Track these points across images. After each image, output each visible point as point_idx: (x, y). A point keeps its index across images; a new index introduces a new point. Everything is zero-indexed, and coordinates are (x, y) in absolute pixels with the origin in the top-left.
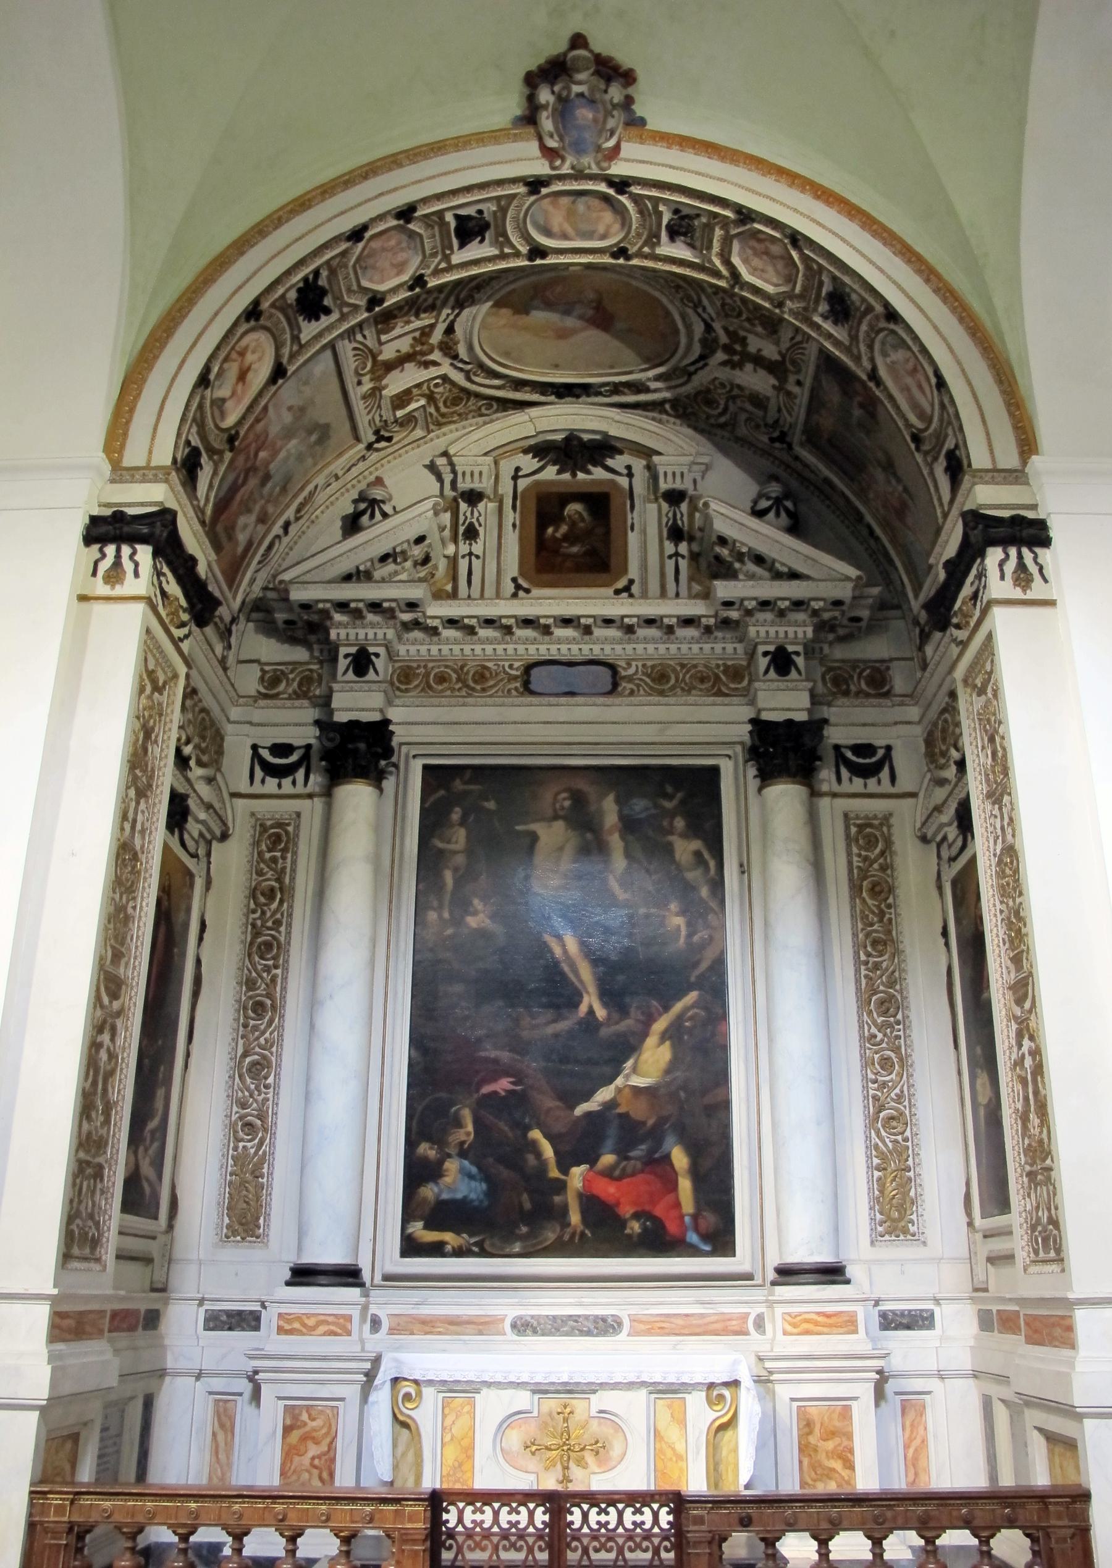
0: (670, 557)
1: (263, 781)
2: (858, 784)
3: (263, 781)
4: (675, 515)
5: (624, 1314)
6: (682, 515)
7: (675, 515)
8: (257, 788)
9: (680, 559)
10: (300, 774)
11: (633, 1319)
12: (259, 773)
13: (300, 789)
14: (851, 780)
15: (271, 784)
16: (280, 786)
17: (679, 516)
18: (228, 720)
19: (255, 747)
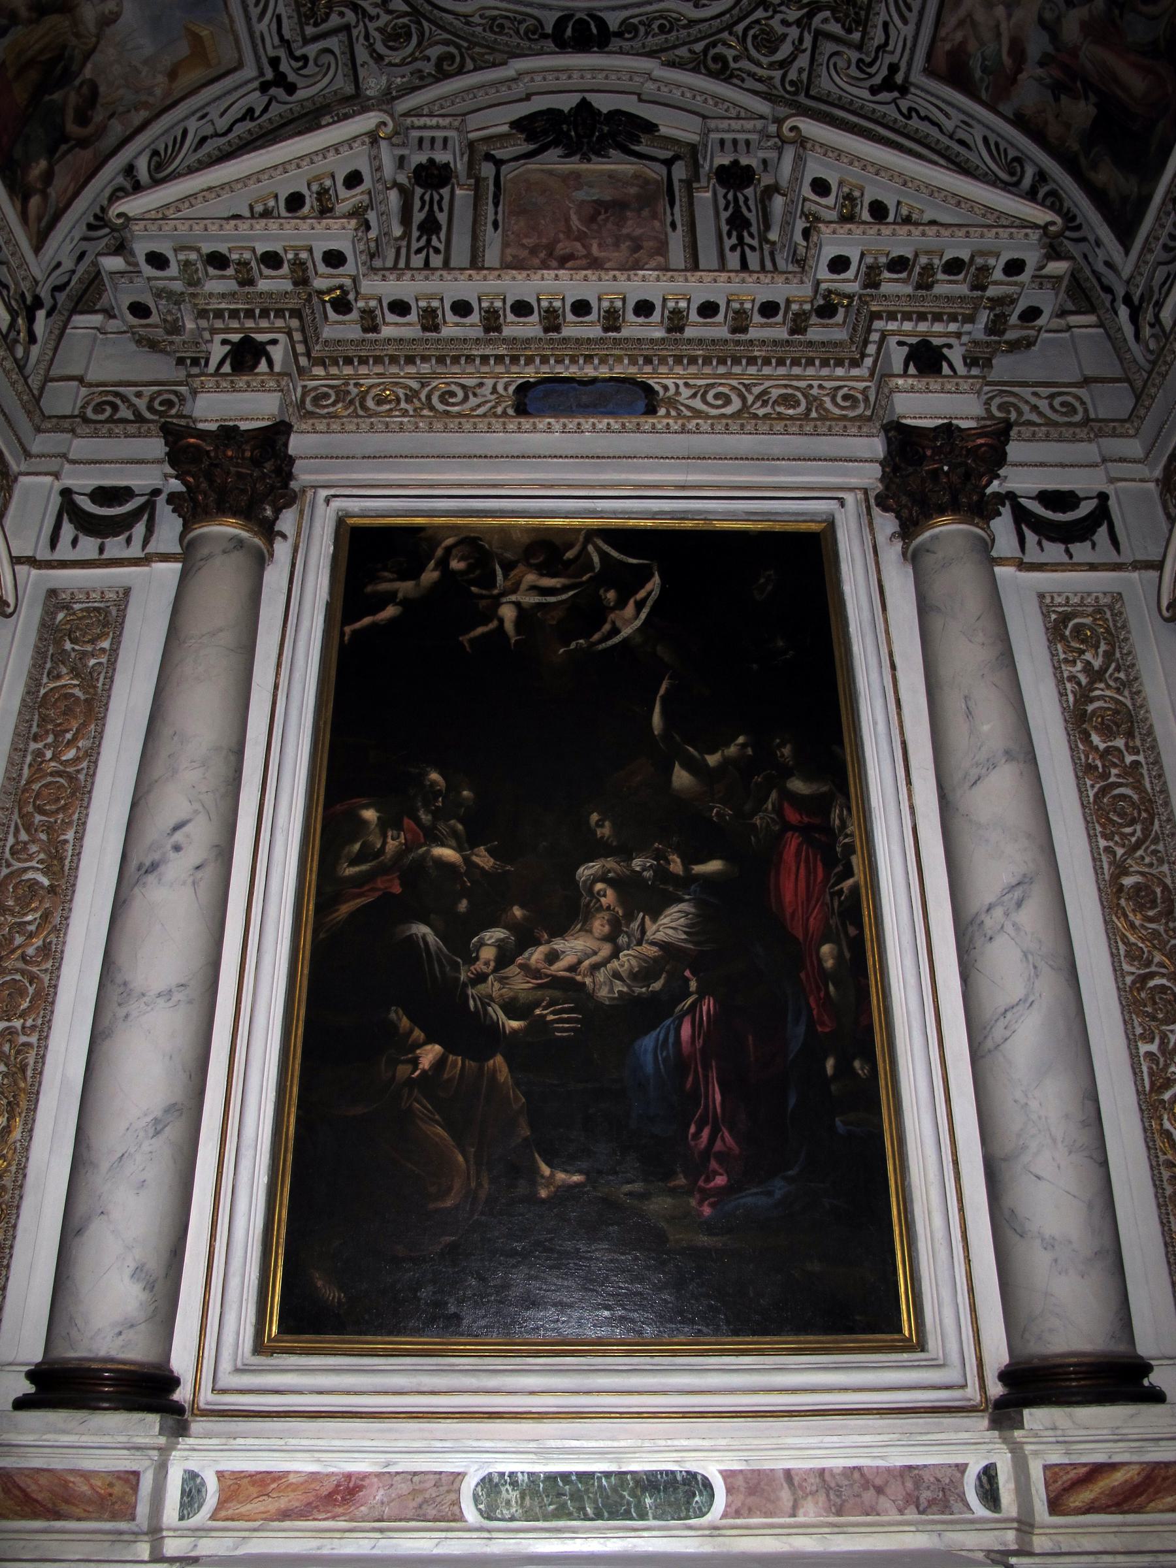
0: (733, 249)
1: (75, 542)
2: (1054, 551)
3: (75, 542)
4: (736, 199)
5: (712, 1470)
6: (746, 199)
7: (736, 199)
8: (64, 551)
9: (747, 250)
10: (139, 529)
11: (727, 1475)
12: (68, 531)
13: (135, 551)
14: (1040, 543)
15: (88, 547)
16: (101, 550)
17: (741, 199)
18: (28, 454)
19: (66, 493)
